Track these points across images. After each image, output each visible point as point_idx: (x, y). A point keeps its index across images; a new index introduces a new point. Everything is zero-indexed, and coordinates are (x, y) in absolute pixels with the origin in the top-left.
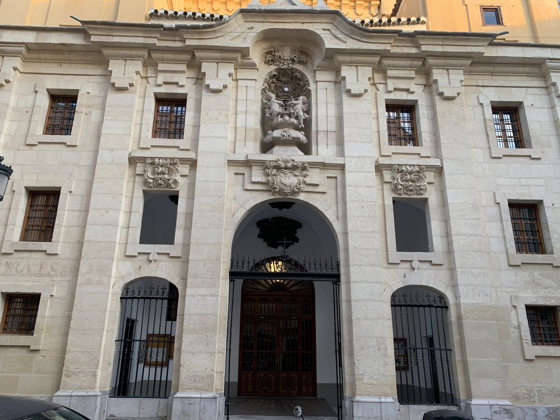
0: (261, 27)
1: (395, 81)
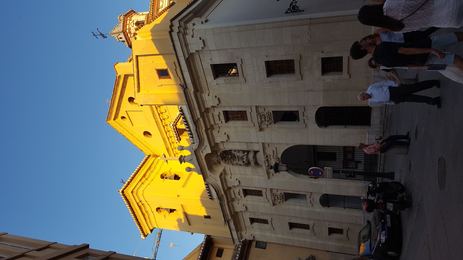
0: (208, 173)
1: (216, 120)
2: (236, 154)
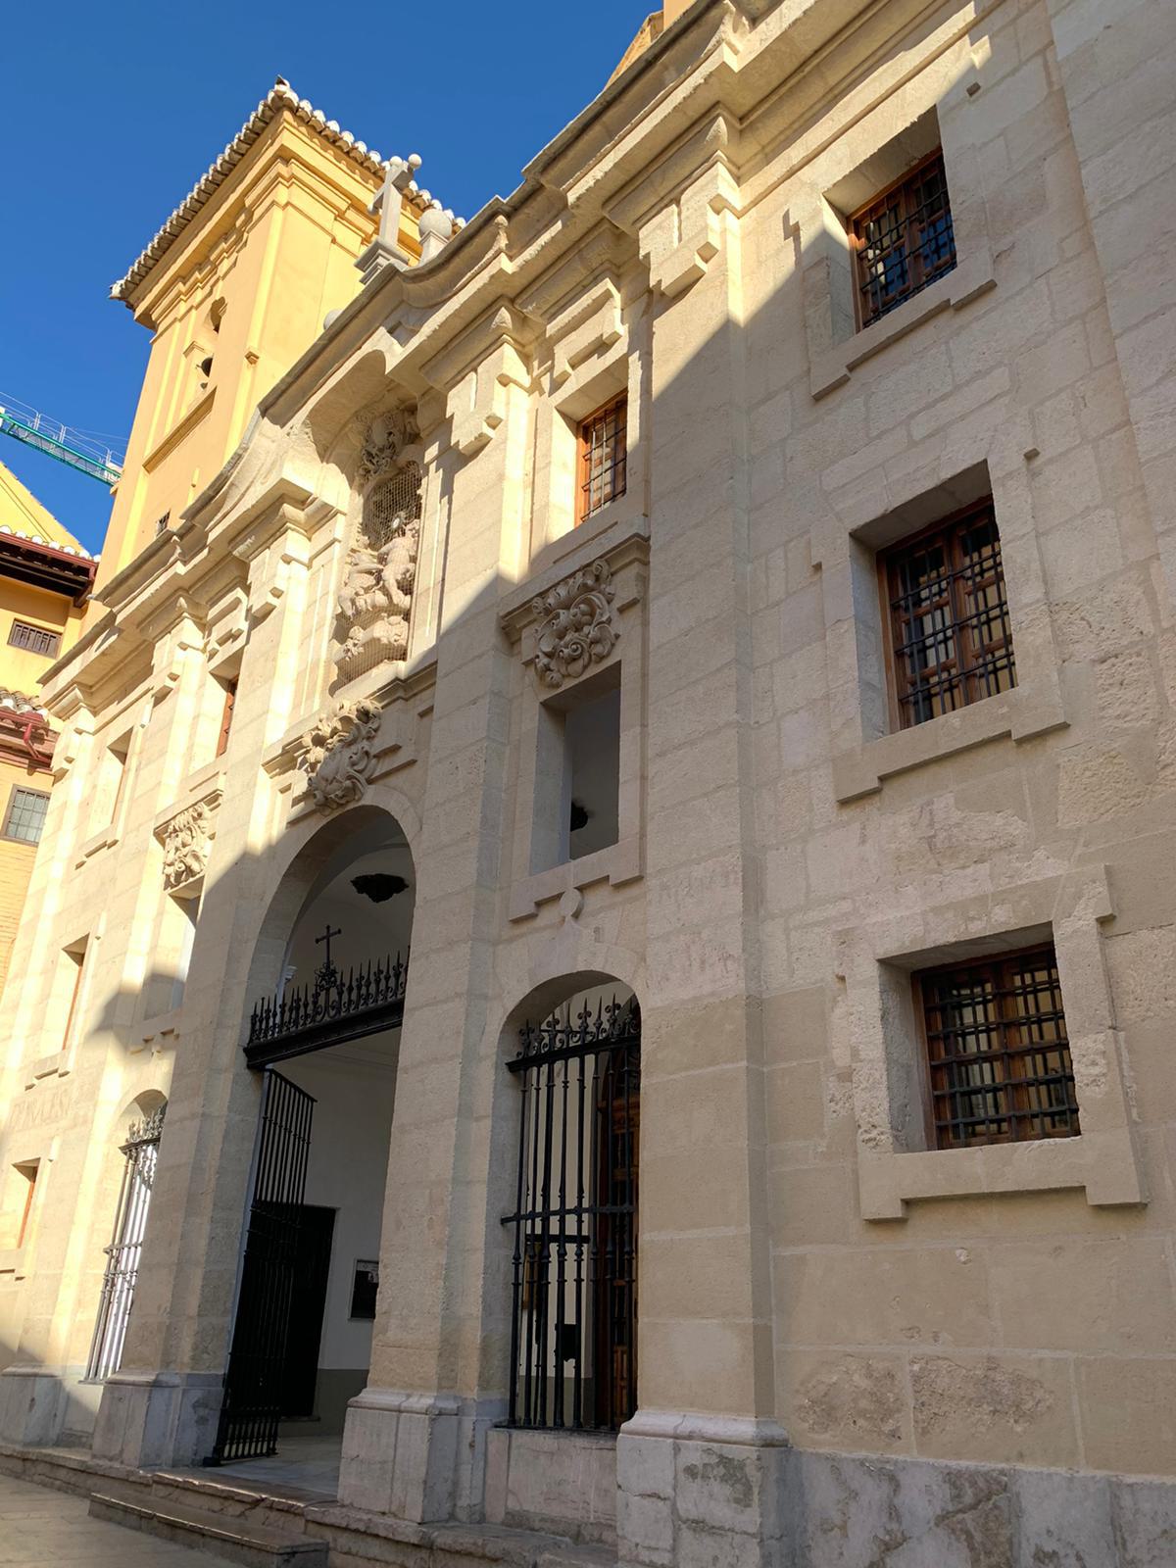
2: (400, 547)
